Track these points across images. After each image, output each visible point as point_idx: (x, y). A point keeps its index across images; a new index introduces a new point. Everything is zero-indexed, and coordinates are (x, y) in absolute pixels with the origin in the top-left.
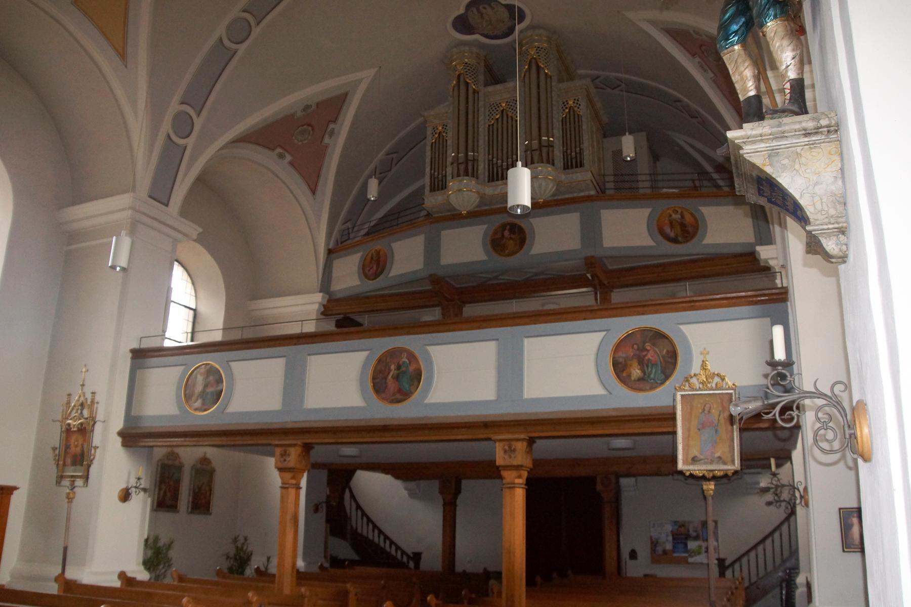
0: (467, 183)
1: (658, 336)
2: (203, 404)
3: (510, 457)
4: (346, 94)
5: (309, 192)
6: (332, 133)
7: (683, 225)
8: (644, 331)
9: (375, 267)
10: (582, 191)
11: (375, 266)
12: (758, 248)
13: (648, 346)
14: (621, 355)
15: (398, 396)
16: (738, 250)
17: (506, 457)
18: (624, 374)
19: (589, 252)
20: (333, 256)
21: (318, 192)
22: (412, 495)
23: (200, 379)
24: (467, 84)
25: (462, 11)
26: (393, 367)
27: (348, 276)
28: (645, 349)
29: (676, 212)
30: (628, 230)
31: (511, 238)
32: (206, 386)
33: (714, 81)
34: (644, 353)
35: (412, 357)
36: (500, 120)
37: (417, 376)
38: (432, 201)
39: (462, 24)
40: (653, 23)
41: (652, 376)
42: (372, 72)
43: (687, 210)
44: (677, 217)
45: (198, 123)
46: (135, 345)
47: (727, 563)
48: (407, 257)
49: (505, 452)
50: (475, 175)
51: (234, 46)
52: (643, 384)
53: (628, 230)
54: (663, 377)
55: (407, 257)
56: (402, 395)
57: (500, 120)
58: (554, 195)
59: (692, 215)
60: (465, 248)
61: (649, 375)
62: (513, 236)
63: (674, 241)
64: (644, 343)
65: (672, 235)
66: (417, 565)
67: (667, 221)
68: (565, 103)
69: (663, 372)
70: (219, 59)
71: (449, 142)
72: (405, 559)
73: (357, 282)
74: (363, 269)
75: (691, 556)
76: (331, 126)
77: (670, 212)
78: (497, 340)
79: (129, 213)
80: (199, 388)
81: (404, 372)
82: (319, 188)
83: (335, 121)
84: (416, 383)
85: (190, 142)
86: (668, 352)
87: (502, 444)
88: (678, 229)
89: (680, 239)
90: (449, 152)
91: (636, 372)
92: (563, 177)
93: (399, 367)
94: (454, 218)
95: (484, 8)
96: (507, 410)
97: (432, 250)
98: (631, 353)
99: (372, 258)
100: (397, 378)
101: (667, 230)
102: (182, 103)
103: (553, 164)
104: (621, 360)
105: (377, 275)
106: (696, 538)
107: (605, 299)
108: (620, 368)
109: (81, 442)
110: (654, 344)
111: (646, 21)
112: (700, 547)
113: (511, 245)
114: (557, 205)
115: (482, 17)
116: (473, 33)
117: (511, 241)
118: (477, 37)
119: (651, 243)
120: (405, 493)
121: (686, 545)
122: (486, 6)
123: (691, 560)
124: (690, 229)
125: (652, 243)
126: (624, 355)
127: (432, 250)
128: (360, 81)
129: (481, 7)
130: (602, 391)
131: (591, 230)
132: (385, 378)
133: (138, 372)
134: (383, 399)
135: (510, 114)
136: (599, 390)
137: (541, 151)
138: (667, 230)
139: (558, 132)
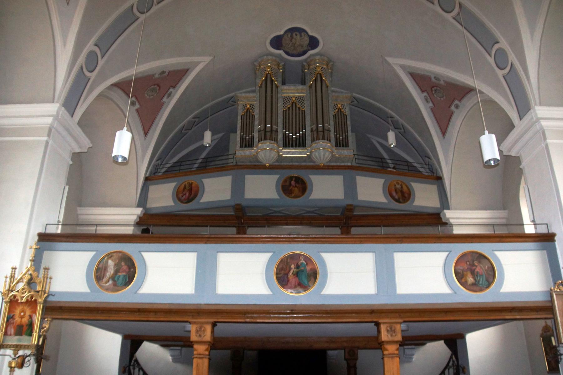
0: (267, 144)
1: (481, 257)
2: (115, 284)
3: (392, 335)
4: (188, 70)
5: (142, 133)
6: (169, 95)
7: (402, 192)
9: (187, 194)
10: (343, 162)
11: (189, 193)
13: (476, 263)
14: (460, 268)
16: (430, 211)
17: (389, 336)
18: (463, 281)
19: (349, 202)
20: (149, 182)
22: (175, 360)
23: (111, 263)
25: (282, 33)
26: (293, 266)
27: (163, 197)
28: (474, 265)
29: (398, 183)
30: (372, 190)
31: (296, 186)
32: (116, 272)
33: (432, 109)
34: (474, 268)
35: (308, 260)
36: (291, 109)
38: (244, 154)
39: (277, 42)
40: (403, 67)
41: (481, 282)
42: (207, 59)
43: (404, 183)
44: (398, 186)
45: (101, 62)
46: (42, 230)
48: (216, 190)
49: (388, 331)
50: (276, 140)
51: (138, 14)
53: (372, 190)
54: (487, 283)
55: (216, 190)
57: (291, 109)
58: (330, 161)
59: (407, 186)
60: (262, 189)
61: (479, 281)
62: (297, 185)
63: (398, 201)
64: (473, 261)
65: (397, 197)
67: (393, 188)
68: (336, 105)
69: (487, 280)
70: (126, 20)
71: (256, 117)
73: (171, 203)
74: (177, 195)
76: (171, 90)
77: (395, 183)
78: (375, 252)
79: (50, 120)
80: (110, 271)
81: (303, 271)
82: (151, 131)
83: (174, 87)
84: (313, 279)
85: (93, 75)
86: (488, 268)
87: (386, 325)
88: (400, 194)
89: (401, 200)
90: (256, 122)
91: (470, 280)
92: (335, 151)
93: (298, 267)
95: (296, 35)
96: (384, 301)
97: (238, 187)
98: (466, 267)
99: (185, 188)
100: (297, 274)
101: (394, 194)
102: (96, 45)
103: (330, 141)
104: (460, 271)
105: (189, 200)
107: (348, 233)
108: (460, 276)
109: (28, 313)
110: (480, 262)
111: (400, 65)
114: (328, 169)
115: (291, 41)
116: (280, 49)
117: (296, 189)
118: (281, 52)
120: (170, 358)
122: (297, 33)
124: (406, 195)
126: (461, 268)
127: (238, 187)
128: (199, 63)
129: (294, 34)
131: (350, 188)
132: (287, 274)
133: (46, 254)
135: (298, 106)
136: (446, 290)
137: (323, 132)
138: (394, 194)
139: (332, 122)
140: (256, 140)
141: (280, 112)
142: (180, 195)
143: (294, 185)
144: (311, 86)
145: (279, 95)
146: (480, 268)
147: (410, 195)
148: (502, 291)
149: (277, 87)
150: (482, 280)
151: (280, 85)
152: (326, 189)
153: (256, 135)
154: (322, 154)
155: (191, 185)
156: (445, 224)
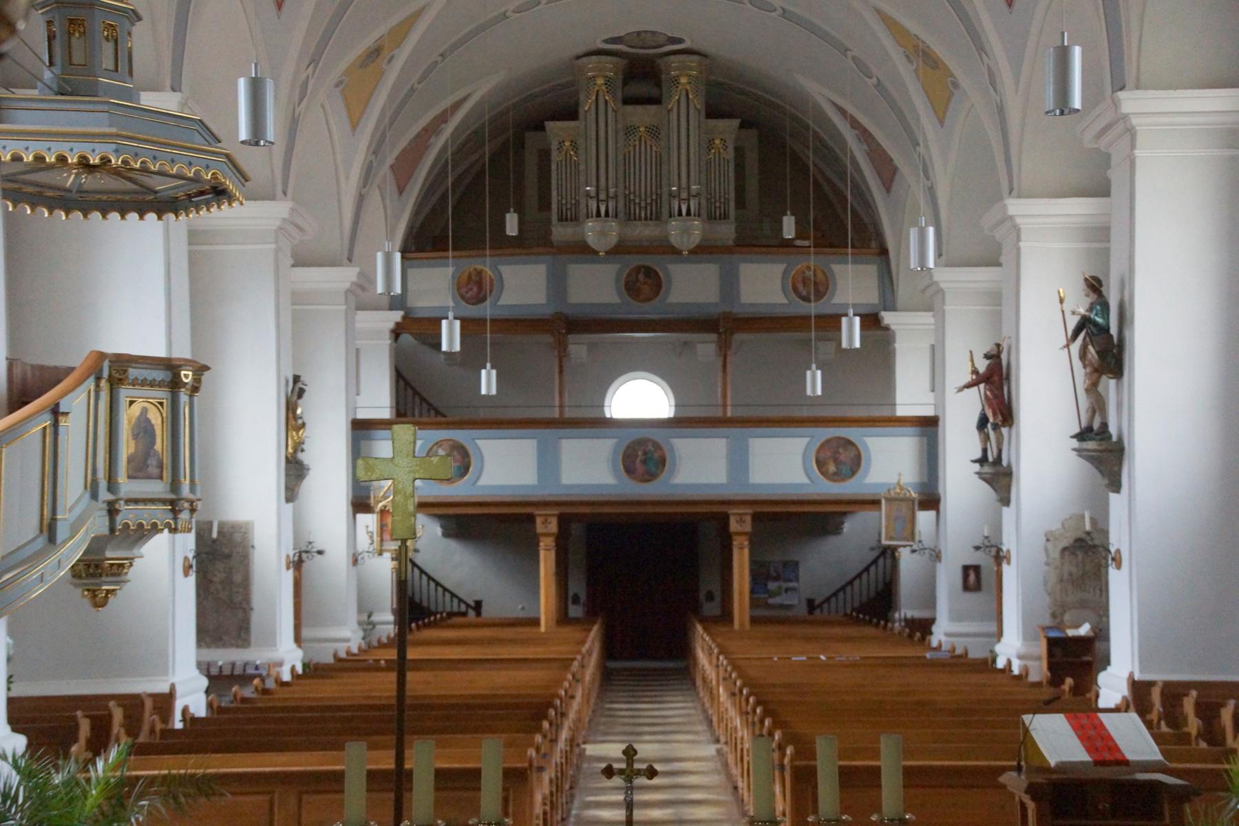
1: (849, 443)
9: (475, 289)
12: (883, 314)
13: (841, 450)
15: (647, 477)
21: (404, 194)
22: (446, 534)
24: (606, 102)
25: (622, 34)
26: (640, 453)
31: (645, 283)
35: (657, 446)
37: (662, 462)
48: (522, 285)
52: (837, 477)
56: (649, 477)
59: (824, 273)
60: (595, 286)
63: (806, 299)
65: (804, 293)
66: (479, 614)
71: (582, 167)
72: (463, 608)
74: (459, 289)
75: (770, 596)
90: (582, 179)
91: (832, 468)
93: (645, 453)
94: (583, 250)
97: (557, 283)
100: (644, 462)
106: (777, 579)
108: (821, 464)
112: (780, 588)
113: (646, 289)
117: (646, 287)
121: (766, 585)
123: (771, 601)
124: (821, 289)
130: (806, 481)
131: (729, 284)
134: (635, 478)
138: (801, 287)
140: (583, 211)
142: (464, 290)
143: (644, 282)
146: (845, 456)
150: (845, 469)
152: (691, 286)
153: (583, 202)
155: (480, 273)
156: (887, 328)
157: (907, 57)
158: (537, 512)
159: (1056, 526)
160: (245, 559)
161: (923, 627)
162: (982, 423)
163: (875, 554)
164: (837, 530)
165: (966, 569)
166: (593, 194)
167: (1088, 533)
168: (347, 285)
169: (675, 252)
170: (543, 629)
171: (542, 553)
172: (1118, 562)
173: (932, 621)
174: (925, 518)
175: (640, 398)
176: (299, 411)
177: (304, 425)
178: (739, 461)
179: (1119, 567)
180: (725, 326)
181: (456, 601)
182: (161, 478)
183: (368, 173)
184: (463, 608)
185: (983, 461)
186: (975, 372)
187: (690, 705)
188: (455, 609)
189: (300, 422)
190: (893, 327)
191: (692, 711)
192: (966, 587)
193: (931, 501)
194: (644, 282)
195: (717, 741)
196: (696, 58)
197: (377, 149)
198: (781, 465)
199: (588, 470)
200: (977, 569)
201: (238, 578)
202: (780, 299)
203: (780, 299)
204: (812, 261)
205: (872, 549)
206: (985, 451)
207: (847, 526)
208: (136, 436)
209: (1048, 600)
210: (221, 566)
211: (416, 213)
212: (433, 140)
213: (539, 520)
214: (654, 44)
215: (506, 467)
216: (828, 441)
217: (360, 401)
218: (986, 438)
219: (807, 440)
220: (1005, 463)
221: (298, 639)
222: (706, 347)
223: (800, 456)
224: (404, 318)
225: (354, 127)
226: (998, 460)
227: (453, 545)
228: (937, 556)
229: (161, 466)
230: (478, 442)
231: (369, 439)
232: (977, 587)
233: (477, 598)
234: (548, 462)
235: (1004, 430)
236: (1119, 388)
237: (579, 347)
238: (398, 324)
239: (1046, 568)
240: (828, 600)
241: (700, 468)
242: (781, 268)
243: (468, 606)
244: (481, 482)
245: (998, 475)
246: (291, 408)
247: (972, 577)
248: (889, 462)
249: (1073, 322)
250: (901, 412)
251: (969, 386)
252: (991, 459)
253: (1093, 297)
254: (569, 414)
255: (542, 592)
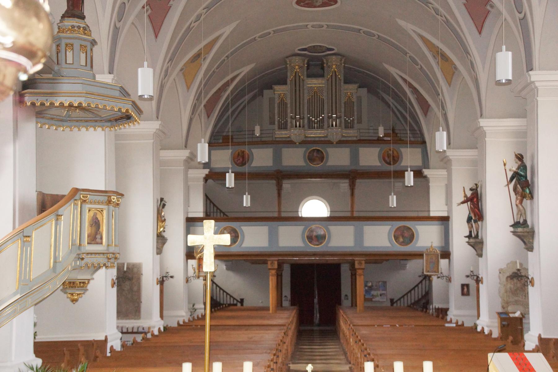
8: (404, 226)
9: (241, 160)
12: (424, 170)
19: (353, 168)
21: (210, 118)
22: (228, 269)
24: (300, 76)
47: (395, 301)
52: (404, 243)
60: (294, 158)
65: (388, 161)
66: (242, 305)
67: (386, 155)
71: (289, 105)
90: (289, 111)
94: (289, 143)
96: (358, 249)
97: (277, 157)
98: (400, 233)
99: (239, 155)
101: (387, 159)
108: (396, 238)
119: (379, 164)
120: (224, 267)
123: (373, 300)
124: (396, 159)
125: (379, 164)
131: (355, 157)
138: (387, 159)
140: (289, 125)
141: (306, 101)
142: (236, 160)
143: (315, 156)
144: (328, 80)
145: (305, 87)
146: (406, 234)
147: (398, 158)
148: (417, 245)
149: (303, 80)
151: (305, 78)
152: (339, 158)
153: (289, 120)
154: (335, 137)
155: (243, 152)
156: (425, 177)
157: (434, 56)
158: (268, 259)
159: (503, 266)
160: (139, 280)
161: (443, 312)
162: (469, 220)
163: (421, 278)
164: (404, 267)
165: (463, 286)
166: (293, 117)
167: (519, 270)
168: (185, 158)
169: (329, 143)
170: (271, 311)
171: (270, 277)
172: (532, 283)
173: (447, 310)
174: (443, 262)
175: (314, 208)
176: (163, 214)
177: (165, 220)
178: (359, 236)
179: (533, 285)
180: (353, 176)
181: (232, 299)
182: (101, 243)
183: (194, 109)
184: (235, 302)
185: (470, 236)
186: (466, 196)
187: (338, 347)
188: (232, 302)
189: (163, 219)
190: (428, 176)
191: (338, 350)
192: (463, 294)
193: (446, 254)
194: (315, 156)
195: (350, 363)
196: (340, 57)
197: (198, 98)
198: (378, 237)
199: (290, 239)
200: (467, 286)
201: (135, 289)
202: (378, 164)
203: (378, 164)
204: (392, 146)
205: (420, 276)
206: (470, 232)
207: (408, 266)
208: (91, 226)
209: (500, 300)
210: (127, 282)
211: (215, 126)
212: (222, 94)
213: (269, 262)
214: (320, 51)
215: (255, 238)
216: (400, 227)
217: (190, 209)
218: (471, 227)
219: (390, 227)
220: (480, 237)
221: (162, 316)
222: (344, 185)
223: (387, 234)
224: (209, 172)
225: (188, 88)
226: (477, 236)
227: (231, 274)
228: (449, 280)
229: (101, 238)
230: (242, 227)
231: (194, 226)
232: (468, 294)
233: (242, 298)
234: (273, 236)
235: (480, 223)
236: (531, 203)
237: (287, 185)
238: (207, 175)
239: (499, 285)
240: (400, 299)
241: (342, 239)
242: (378, 149)
243: (237, 301)
244: (244, 245)
245: (476, 242)
246: (159, 213)
247: (466, 290)
248: (427, 237)
249: (510, 174)
250: (432, 214)
251: (463, 203)
252: (473, 236)
253: (520, 163)
254: (283, 215)
255: (271, 295)
